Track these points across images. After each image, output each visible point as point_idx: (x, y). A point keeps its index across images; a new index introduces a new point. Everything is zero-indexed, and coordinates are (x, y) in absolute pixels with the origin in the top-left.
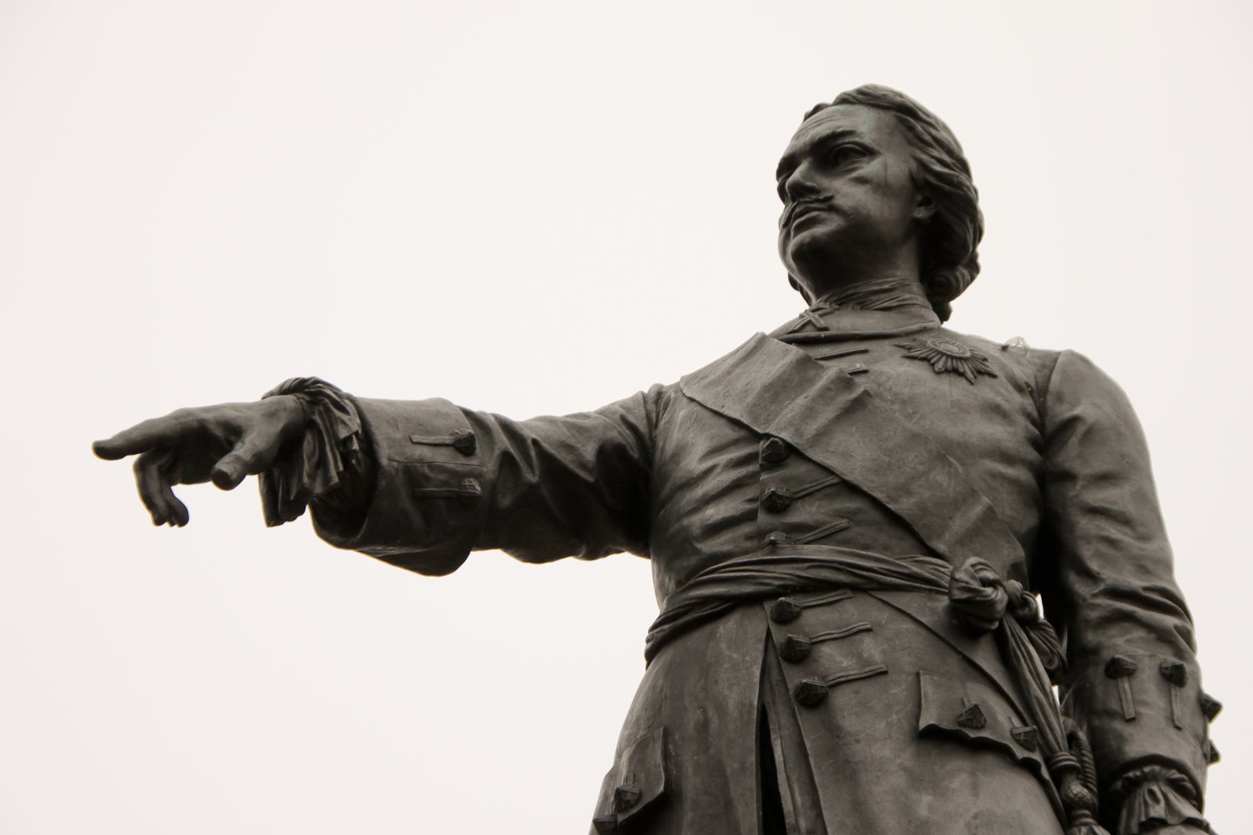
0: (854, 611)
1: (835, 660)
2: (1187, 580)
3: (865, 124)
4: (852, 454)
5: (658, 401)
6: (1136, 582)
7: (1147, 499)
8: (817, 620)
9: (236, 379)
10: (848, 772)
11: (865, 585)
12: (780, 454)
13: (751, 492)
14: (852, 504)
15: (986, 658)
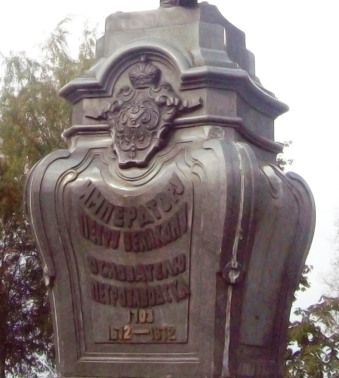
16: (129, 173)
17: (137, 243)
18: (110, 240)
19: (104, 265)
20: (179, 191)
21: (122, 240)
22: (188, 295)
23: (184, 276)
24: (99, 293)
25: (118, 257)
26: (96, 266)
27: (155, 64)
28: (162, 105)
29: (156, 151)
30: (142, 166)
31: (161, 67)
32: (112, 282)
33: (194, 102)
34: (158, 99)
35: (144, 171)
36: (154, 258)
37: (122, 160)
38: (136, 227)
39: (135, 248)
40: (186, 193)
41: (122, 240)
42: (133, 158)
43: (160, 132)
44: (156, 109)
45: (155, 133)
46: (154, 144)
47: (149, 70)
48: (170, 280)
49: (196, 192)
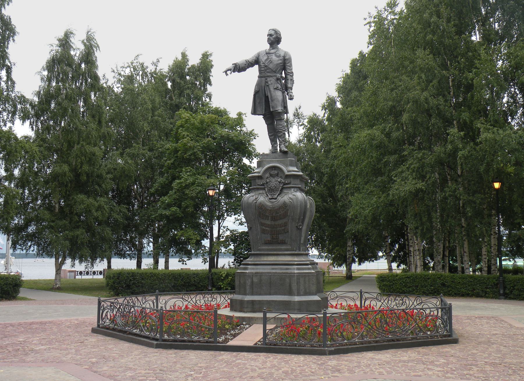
0: (271, 78)
1: (269, 83)
2: (293, 71)
3: (273, 32)
4: (271, 66)
5: (259, 55)
6: (290, 71)
7: (291, 64)
8: (268, 79)
9: (230, 66)
10: (270, 91)
11: (271, 77)
12: (266, 66)
15: (279, 82)
17: (274, 219)
19: (265, 224)
24: (263, 231)
25: (268, 222)
26: (262, 224)
28: (279, 182)
29: (279, 194)
30: (276, 199)
33: (289, 182)
34: (279, 180)
37: (270, 197)
46: (278, 193)
47: (276, 172)
48: (283, 228)
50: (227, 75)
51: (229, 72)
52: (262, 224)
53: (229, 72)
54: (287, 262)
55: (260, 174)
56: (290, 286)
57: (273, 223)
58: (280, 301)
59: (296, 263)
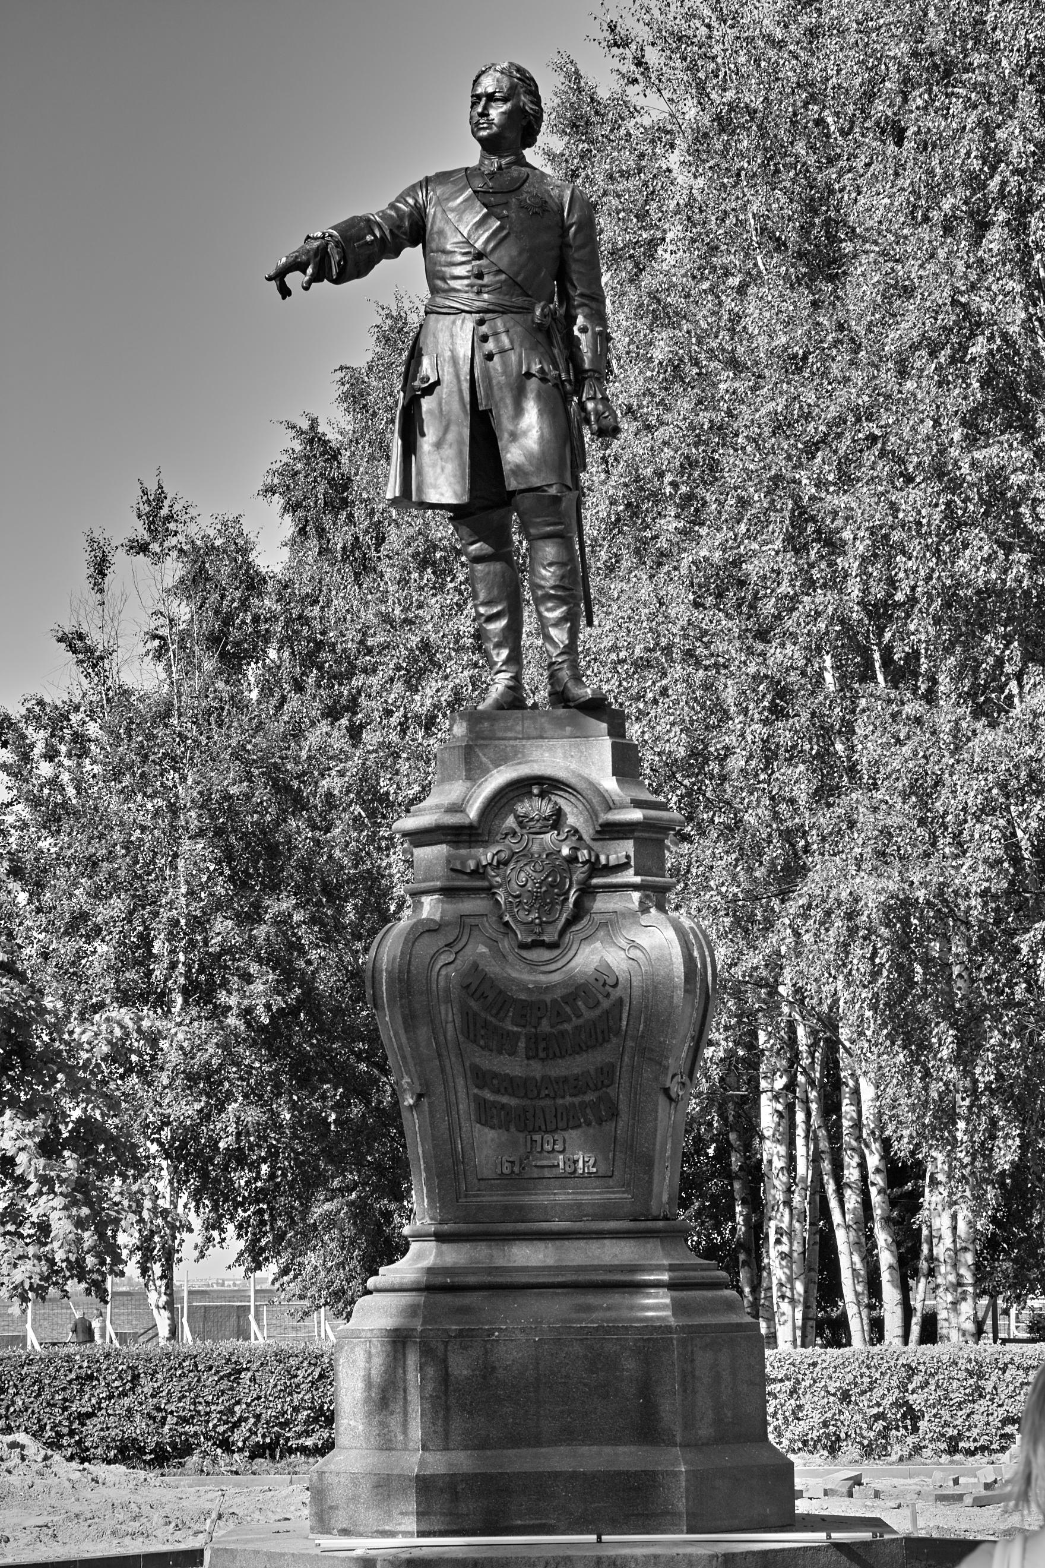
13: (468, 267)
14: (503, 277)
16: (534, 955)
18: (504, 1043)
19: (495, 1075)
20: (611, 981)
21: (522, 1044)
22: (614, 1114)
23: (611, 1092)
25: (513, 1066)
26: (481, 1078)
27: (553, 797)
28: (572, 860)
29: (569, 923)
31: (562, 802)
32: (505, 1100)
35: (556, 952)
36: (560, 1068)
38: (545, 1026)
39: (542, 1055)
40: (620, 986)
41: (522, 1044)
42: (540, 934)
43: (572, 900)
44: (565, 866)
45: (566, 899)
49: (635, 984)
50: (285, 292)
51: (294, 280)
52: (481, 1078)
53: (294, 280)
54: (582, 1278)
55: (467, 821)
56: (646, 1389)
57: (537, 1070)
58: (594, 1475)
59: (665, 1277)
